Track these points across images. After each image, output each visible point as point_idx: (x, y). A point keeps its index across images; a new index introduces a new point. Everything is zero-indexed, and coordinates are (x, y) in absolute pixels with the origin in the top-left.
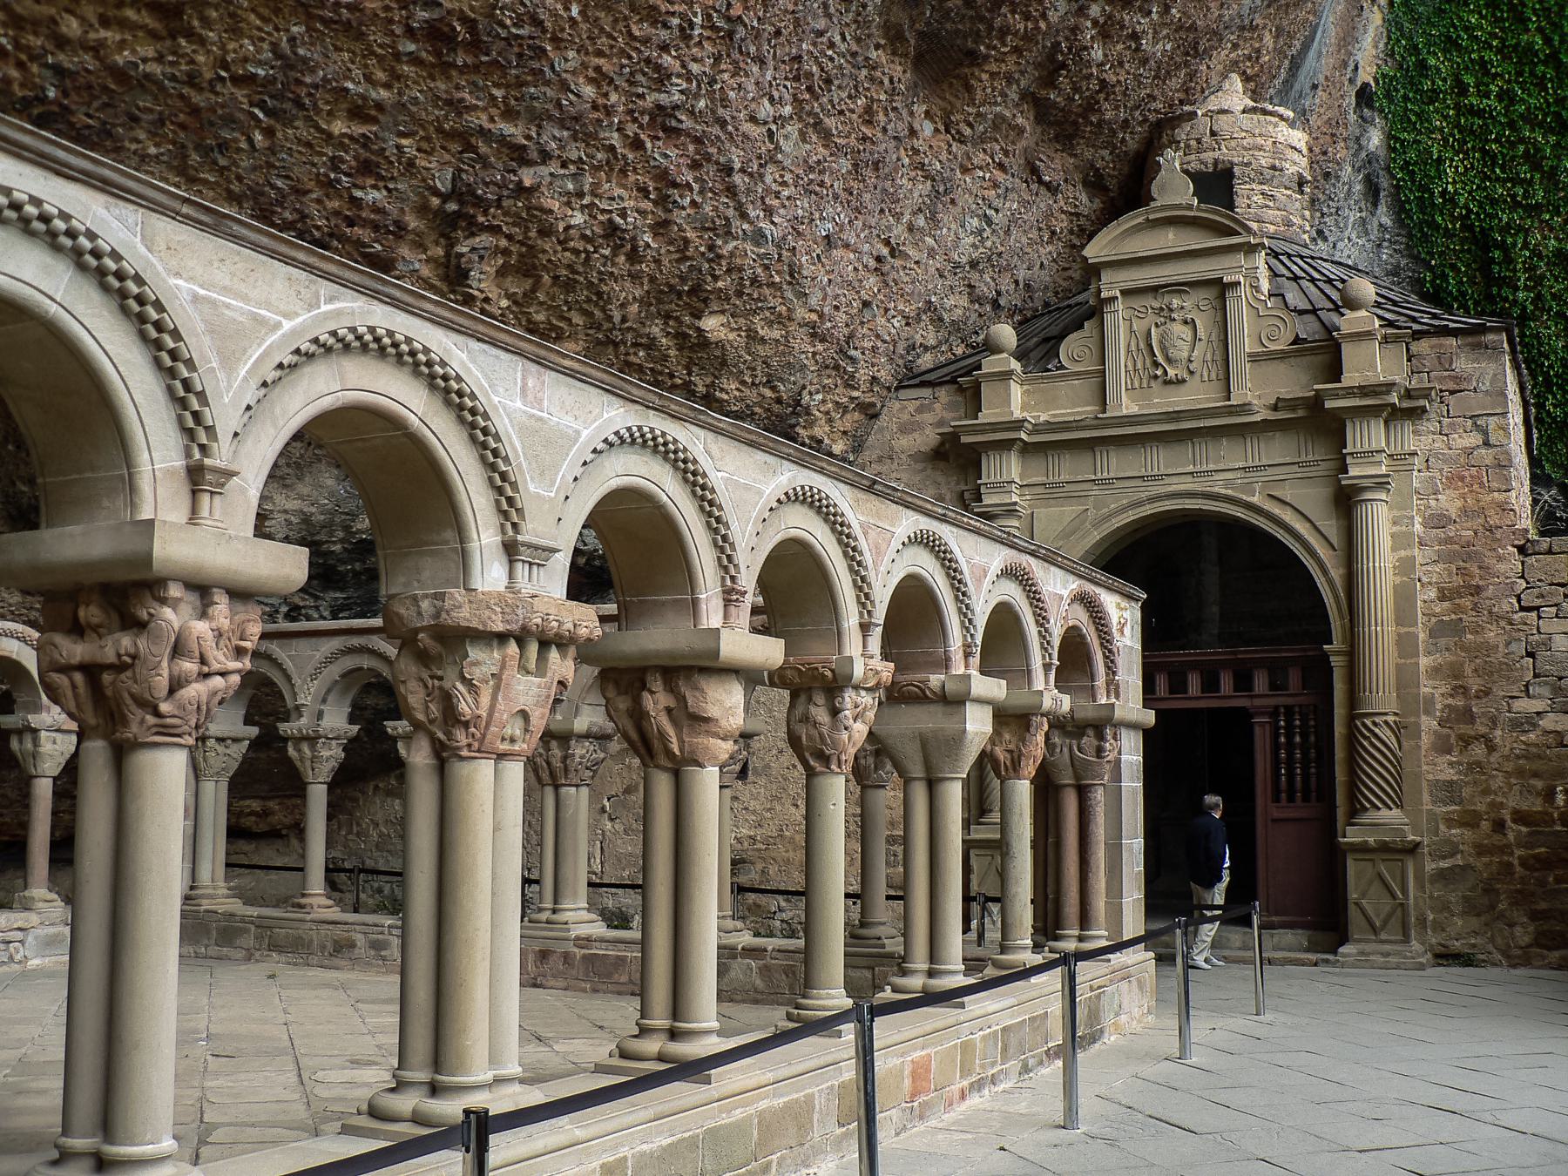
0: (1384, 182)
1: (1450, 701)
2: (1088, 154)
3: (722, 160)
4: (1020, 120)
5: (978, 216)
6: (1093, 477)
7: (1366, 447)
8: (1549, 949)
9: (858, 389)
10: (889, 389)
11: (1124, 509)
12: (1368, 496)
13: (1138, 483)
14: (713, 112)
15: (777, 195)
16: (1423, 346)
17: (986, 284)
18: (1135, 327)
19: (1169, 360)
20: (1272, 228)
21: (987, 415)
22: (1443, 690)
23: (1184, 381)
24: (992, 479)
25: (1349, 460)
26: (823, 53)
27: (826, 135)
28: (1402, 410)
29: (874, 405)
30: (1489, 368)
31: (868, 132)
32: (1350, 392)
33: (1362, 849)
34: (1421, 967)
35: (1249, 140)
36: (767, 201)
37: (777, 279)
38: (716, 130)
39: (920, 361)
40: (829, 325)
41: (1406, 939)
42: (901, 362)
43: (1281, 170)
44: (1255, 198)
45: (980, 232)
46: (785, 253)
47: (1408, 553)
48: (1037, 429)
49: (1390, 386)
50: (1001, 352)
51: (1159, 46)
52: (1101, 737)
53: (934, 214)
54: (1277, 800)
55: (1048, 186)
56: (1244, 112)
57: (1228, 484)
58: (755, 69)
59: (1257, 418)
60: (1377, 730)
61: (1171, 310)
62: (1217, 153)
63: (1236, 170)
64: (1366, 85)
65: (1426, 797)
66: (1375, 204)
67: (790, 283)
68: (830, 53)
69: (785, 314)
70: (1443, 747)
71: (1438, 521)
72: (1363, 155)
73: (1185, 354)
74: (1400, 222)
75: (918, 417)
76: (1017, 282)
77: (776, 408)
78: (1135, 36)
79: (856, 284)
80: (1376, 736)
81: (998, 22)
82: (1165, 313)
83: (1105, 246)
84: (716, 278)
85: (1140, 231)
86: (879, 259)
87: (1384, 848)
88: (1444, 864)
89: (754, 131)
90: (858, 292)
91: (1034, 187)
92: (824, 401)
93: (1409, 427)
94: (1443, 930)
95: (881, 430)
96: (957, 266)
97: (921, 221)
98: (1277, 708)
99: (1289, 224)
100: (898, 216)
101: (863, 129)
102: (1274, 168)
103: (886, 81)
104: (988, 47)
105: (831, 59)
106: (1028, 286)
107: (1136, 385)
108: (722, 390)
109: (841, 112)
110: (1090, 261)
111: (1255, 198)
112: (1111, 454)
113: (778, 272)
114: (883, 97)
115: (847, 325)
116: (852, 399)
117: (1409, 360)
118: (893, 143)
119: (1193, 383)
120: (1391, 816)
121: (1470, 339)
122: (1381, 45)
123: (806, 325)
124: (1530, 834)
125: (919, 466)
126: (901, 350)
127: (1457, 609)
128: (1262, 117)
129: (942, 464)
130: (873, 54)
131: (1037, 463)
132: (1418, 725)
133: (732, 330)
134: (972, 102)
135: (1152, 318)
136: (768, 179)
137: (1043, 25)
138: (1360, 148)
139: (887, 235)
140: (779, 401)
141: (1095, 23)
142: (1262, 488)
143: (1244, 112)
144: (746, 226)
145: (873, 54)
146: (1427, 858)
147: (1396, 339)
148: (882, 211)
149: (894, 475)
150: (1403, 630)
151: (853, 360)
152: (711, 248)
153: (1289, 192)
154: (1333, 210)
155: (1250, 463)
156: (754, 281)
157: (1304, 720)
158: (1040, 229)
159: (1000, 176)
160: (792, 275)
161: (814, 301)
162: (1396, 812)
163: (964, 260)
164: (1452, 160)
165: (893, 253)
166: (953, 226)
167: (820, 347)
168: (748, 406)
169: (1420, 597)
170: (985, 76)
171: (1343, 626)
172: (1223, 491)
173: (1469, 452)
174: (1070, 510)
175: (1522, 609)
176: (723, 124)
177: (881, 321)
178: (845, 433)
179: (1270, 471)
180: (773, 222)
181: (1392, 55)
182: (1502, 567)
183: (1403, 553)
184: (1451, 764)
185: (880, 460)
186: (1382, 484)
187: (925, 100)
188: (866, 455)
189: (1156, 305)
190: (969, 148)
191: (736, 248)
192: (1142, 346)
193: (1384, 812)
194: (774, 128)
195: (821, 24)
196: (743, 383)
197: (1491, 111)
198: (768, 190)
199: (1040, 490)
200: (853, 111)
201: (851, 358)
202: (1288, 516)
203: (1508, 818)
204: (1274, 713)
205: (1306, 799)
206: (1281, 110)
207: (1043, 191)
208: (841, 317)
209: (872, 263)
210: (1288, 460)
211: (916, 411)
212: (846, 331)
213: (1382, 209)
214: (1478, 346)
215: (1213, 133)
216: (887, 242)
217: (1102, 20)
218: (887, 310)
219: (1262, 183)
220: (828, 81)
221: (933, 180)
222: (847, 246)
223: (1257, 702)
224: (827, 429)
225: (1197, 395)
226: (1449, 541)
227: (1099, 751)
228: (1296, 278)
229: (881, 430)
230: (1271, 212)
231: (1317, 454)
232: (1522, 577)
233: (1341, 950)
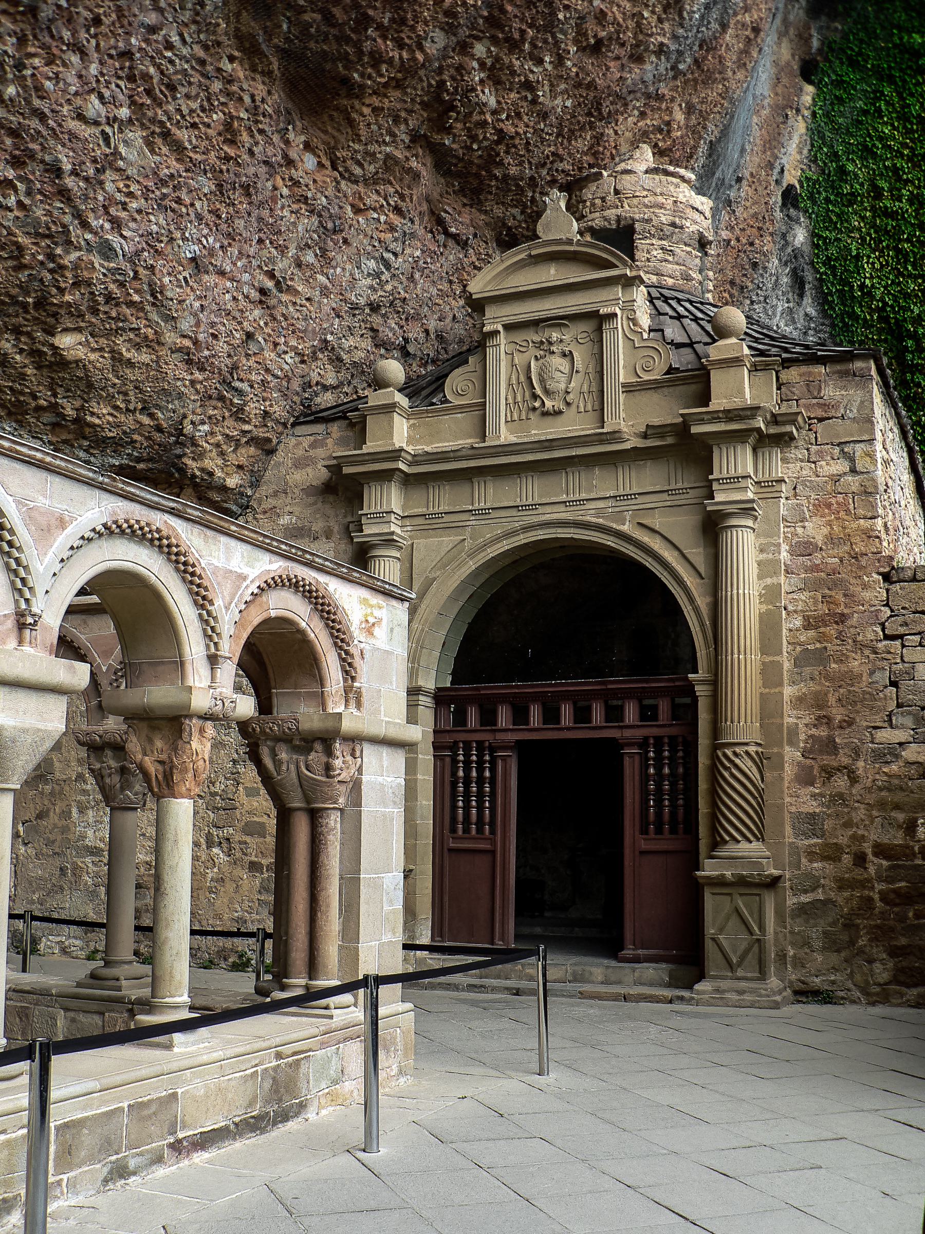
0: (809, 276)
1: (814, 731)
2: (498, 211)
3: (47, 158)
4: (414, 164)
5: (374, 258)
6: (471, 508)
7: (732, 473)
8: (908, 986)
9: (248, 423)
10: (285, 425)
11: (498, 539)
13: (514, 512)
14: (28, 102)
15: (125, 208)
16: (792, 374)
17: (391, 329)
18: (516, 361)
19: (547, 392)
20: (670, 282)
21: (370, 446)
22: (807, 720)
23: (560, 412)
24: (373, 510)
25: (715, 486)
26: (159, 52)
27: (178, 149)
28: (769, 436)
29: (269, 440)
30: (855, 395)
31: (231, 152)
32: (715, 417)
33: (719, 883)
34: (776, 1006)
35: (651, 198)
36: (113, 211)
37: (136, 298)
38: (35, 123)
39: (318, 400)
40: (206, 353)
41: (763, 975)
42: (296, 398)
43: (682, 227)
44: (655, 253)
45: (377, 275)
46: (141, 271)
47: (775, 580)
48: (416, 460)
49: (754, 410)
50: (387, 386)
51: (559, 101)
52: (329, 753)
53: (324, 251)
54: (644, 831)
55: (455, 237)
56: (646, 172)
57: (599, 512)
58: (75, 59)
59: (627, 446)
60: (737, 761)
61: (550, 343)
62: (619, 211)
63: (637, 226)
64: (790, 187)
65: (788, 830)
66: (801, 295)
67: (154, 304)
68: (169, 54)
69: (151, 337)
70: (805, 778)
71: (804, 549)
72: (789, 250)
73: (562, 386)
74: (824, 313)
75: (312, 453)
76: (427, 332)
77: (157, 436)
78: (528, 86)
79: (238, 315)
80: (737, 766)
81: (367, 46)
82: (545, 347)
83: (490, 282)
84: (62, 291)
85: (524, 266)
86: (263, 291)
87: (742, 882)
88: (805, 899)
89: (86, 132)
90: (240, 323)
91: (441, 238)
92: (212, 433)
93: (777, 454)
94: (803, 966)
95: (278, 464)
96: (355, 307)
97: (309, 257)
98: (646, 739)
99: (688, 278)
100: (282, 250)
101: (225, 148)
102: (673, 225)
103: (247, 99)
104: (362, 75)
105: (171, 62)
106: (440, 337)
107: (516, 417)
108: (92, 414)
109: (194, 126)
110: (474, 297)
111: (655, 253)
113: (137, 291)
115: (229, 356)
116: (244, 432)
117: (779, 388)
118: (263, 169)
119: (571, 413)
120: (750, 848)
121: (838, 367)
122: (805, 152)
124: (890, 868)
125: (311, 500)
126: (296, 385)
127: (822, 638)
128: (663, 178)
129: (331, 498)
130: (228, 67)
131: (418, 494)
132: (781, 756)
133: (93, 350)
134: (357, 138)
135: (533, 352)
136: (109, 186)
137: (420, 57)
138: (787, 244)
139: (271, 267)
140: (159, 429)
141: (482, 65)
142: (632, 516)
143: (646, 172)
144: (88, 236)
145: (228, 67)
146: (788, 893)
147: (766, 367)
148: (260, 241)
149: (288, 508)
150: (768, 659)
152: (51, 257)
153: (688, 249)
154: (762, 299)
155: (621, 492)
156: (109, 298)
157: (673, 750)
158: (451, 282)
159: (396, 220)
160: (153, 295)
161: (186, 325)
162: (755, 845)
163: (362, 301)
164: (869, 257)
165: (278, 284)
166: (348, 267)
167: (198, 376)
168: (124, 433)
169: (785, 626)
170: (366, 111)
171: (708, 654)
172: (594, 520)
173: (836, 479)
174: (448, 541)
175: (887, 637)
176: (42, 117)
177: (269, 355)
178: (240, 467)
179: (641, 499)
180: (122, 236)
181: (815, 161)
182: (867, 595)
183: (769, 581)
184: (814, 796)
185: (275, 494)
186: (747, 510)
187: (304, 131)
188: (264, 490)
189: (537, 338)
190: (361, 188)
191: (79, 258)
193: (744, 845)
194: (108, 129)
195: (152, 18)
196: (116, 408)
197: (903, 213)
198: (110, 199)
199: (420, 521)
200: (208, 126)
201: (236, 389)
202: (656, 544)
203: (869, 851)
204: (643, 744)
205: (673, 831)
206: (682, 171)
207: (451, 243)
208: (221, 347)
209: (255, 295)
210: (658, 488)
211: (310, 446)
212: (228, 361)
213: (808, 300)
214: (844, 374)
215: (617, 192)
216: (271, 275)
217: (489, 62)
218: (276, 345)
219: (661, 239)
220: (172, 88)
221: (320, 216)
222: (222, 273)
223: (628, 733)
224: (220, 462)
226: (815, 568)
227: (328, 768)
228: (679, 317)
229: (278, 464)
230: (670, 266)
231: (684, 480)
232: (887, 605)
233: (697, 987)
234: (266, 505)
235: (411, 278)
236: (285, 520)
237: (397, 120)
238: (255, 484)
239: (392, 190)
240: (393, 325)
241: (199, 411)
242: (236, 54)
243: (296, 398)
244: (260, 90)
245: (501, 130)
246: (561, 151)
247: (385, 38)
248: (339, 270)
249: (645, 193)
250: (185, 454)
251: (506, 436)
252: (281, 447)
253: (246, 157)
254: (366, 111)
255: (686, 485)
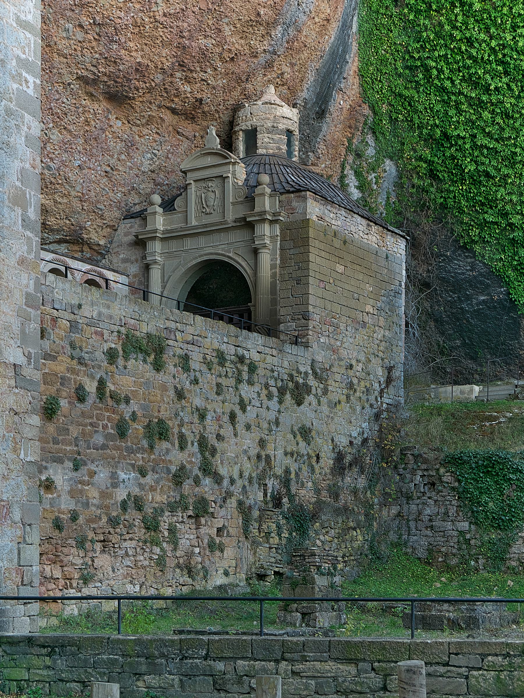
5: (150, 153)
9: (106, 220)
10: (120, 220)
12: (260, 251)
13: (196, 250)
19: (207, 206)
20: (271, 151)
21: (149, 228)
27: (70, 131)
29: (114, 226)
36: (50, 156)
37: (60, 182)
39: (133, 209)
40: (87, 197)
42: (123, 209)
44: (265, 140)
45: (152, 159)
50: (154, 205)
57: (223, 249)
59: (230, 226)
62: (251, 122)
73: (212, 204)
75: (130, 230)
90: (98, 185)
100: (112, 156)
102: (273, 127)
103: (92, 111)
105: (65, 107)
111: (265, 140)
112: (189, 240)
114: (91, 116)
115: (96, 197)
116: (104, 224)
123: (77, 197)
125: (130, 248)
129: (138, 247)
133: (47, 200)
136: (48, 149)
137: (153, 84)
139: (108, 163)
140: (73, 225)
143: (263, 104)
149: (123, 252)
151: (101, 210)
153: (280, 136)
156: (51, 183)
163: (147, 170)
165: (112, 169)
166: (139, 158)
168: (60, 227)
170: (137, 103)
188: (114, 245)
189: (204, 185)
192: (200, 201)
194: (46, 132)
196: (56, 218)
198: (50, 153)
199: (167, 254)
208: (93, 194)
209: (103, 174)
210: (241, 240)
217: (183, 78)
219: (268, 133)
220: (66, 114)
221: (125, 142)
225: (215, 218)
229: (118, 235)
234: (115, 251)
235: (167, 157)
236: (122, 256)
237: (151, 103)
238: (111, 243)
239: (153, 127)
240: (162, 177)
241: (86, 217)
242: (86, 98)
243: (123, 209)
244: (96, 106)
245: (196, 98)
246: (226, 98)
247: (139, 82)
248: (136, 160)
249: (262, 113)
250: (83, 233)
251: (194, 223)
252: (119, 228)
253: (94, 129)
254: (137, 103)
255: (247, 239)
